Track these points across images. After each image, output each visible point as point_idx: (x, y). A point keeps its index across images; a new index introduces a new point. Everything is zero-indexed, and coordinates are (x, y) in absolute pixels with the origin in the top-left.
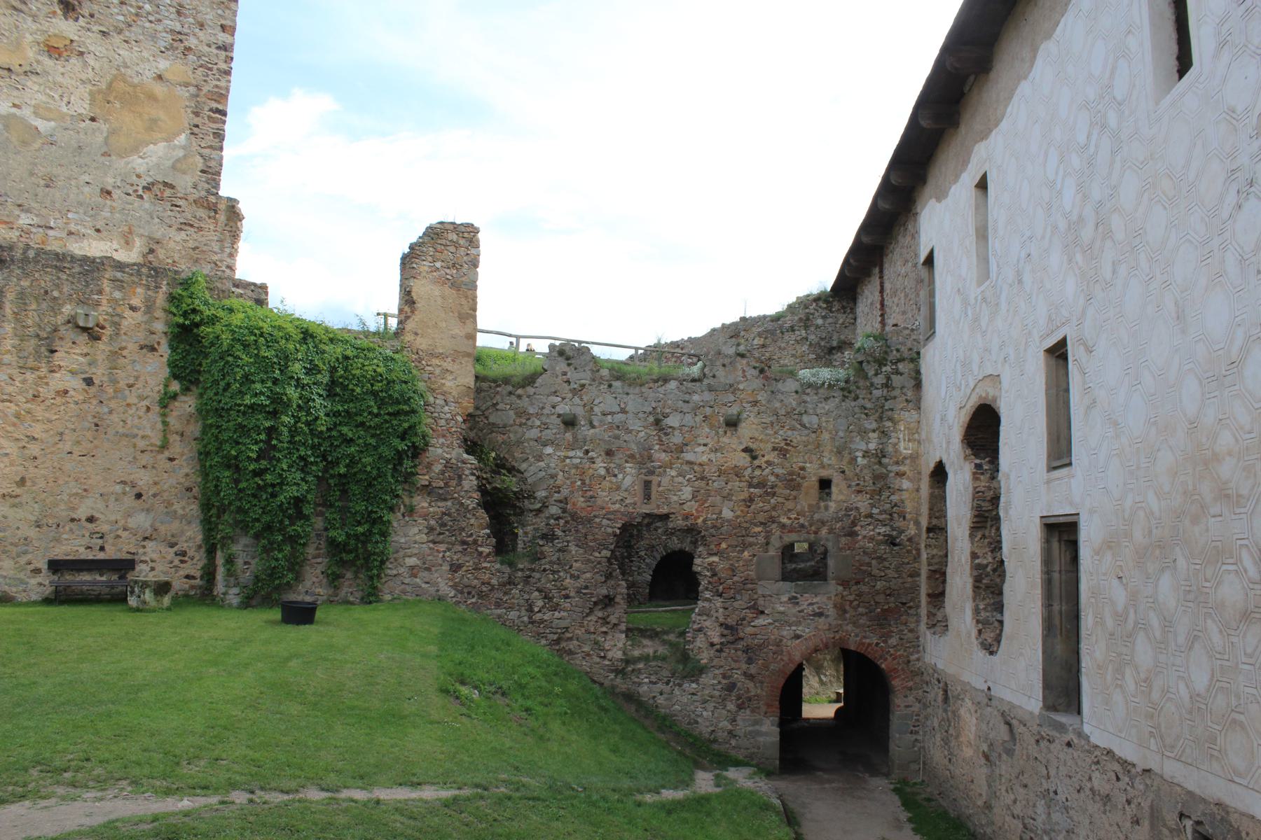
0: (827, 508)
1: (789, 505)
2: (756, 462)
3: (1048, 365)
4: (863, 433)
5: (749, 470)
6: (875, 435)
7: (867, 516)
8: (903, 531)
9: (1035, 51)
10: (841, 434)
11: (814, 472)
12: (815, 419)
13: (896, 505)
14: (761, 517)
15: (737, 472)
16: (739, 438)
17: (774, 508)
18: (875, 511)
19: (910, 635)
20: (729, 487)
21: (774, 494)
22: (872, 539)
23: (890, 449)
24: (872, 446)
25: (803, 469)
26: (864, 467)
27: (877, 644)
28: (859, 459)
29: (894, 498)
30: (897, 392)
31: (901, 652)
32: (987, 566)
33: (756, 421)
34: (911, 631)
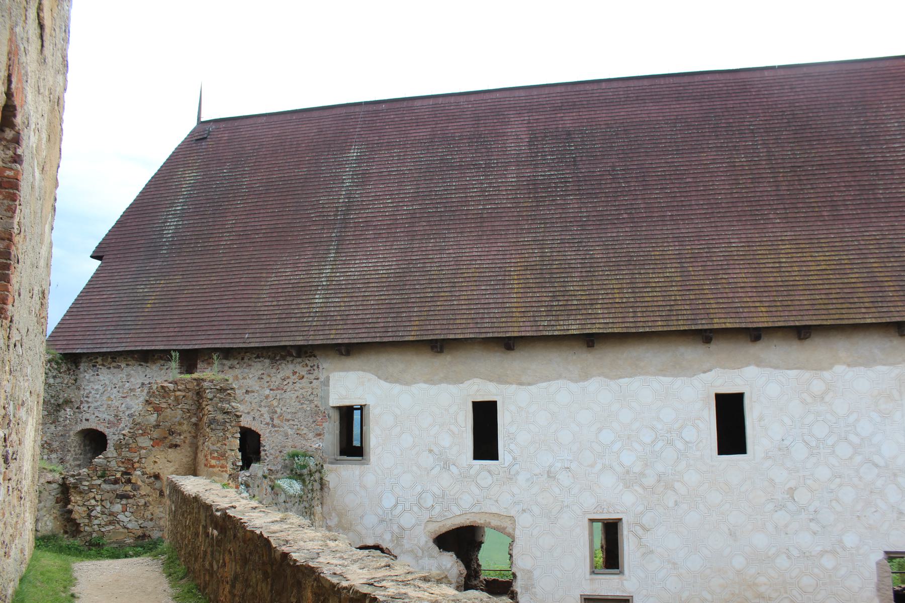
9: (585, 377)
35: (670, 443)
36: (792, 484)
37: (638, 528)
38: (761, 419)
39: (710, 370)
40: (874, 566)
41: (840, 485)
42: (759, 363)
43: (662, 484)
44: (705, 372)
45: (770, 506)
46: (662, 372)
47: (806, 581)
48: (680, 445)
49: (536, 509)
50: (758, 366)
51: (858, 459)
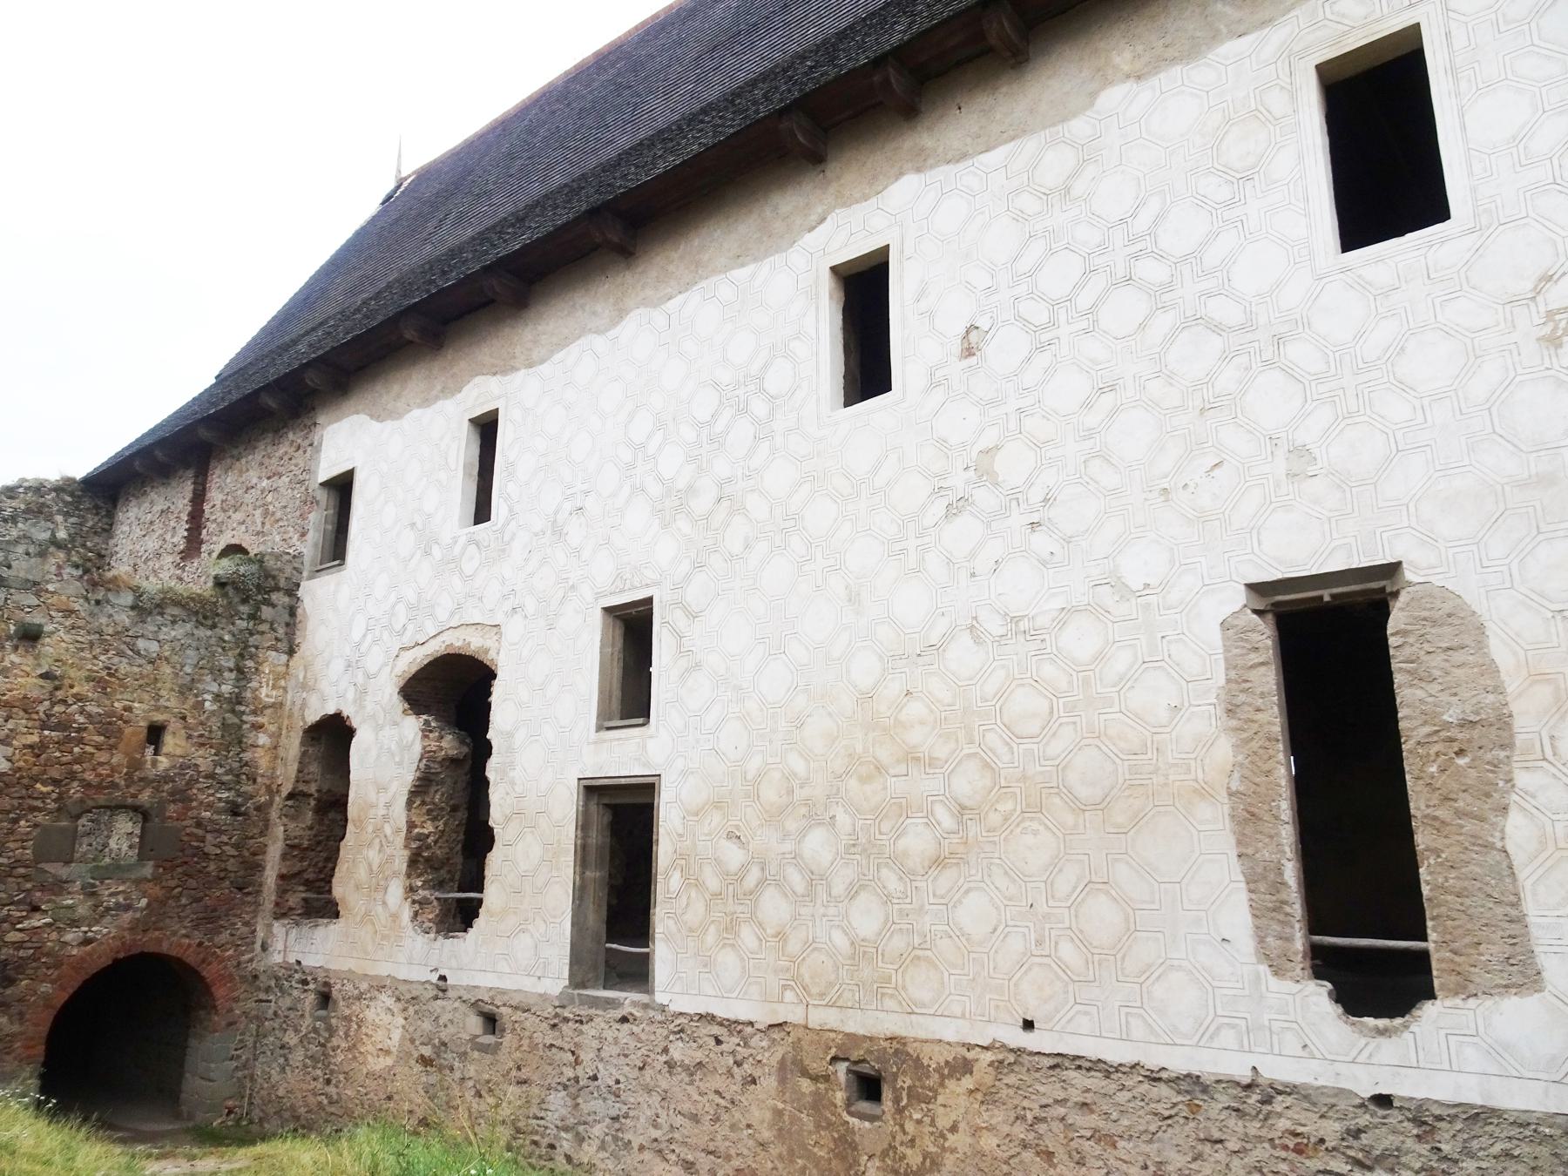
0: (154, 763)
1: (103, 757)
2: (60, 694)
3: (604, 625)
4: (217, 673)
5: (47, 703)
6: (233, 675)
7: (206, 777)
8: (252, 797)
10: (188, 669)
11: (142, 712)
12: (154, 647)
13: (246, 764)
14: (55, 773)
15: (27, 705)
16: (37, 657)
17: (78, 761)
18: (219, 771)
19: (245, 930)
20: (10, 725)
21: (80, 741)
22: (209, 806)
23: (248, 694)
24: (226, 689)
25: (128, 709)
26: (213, 713)
27: (200, 944)
28: (207, 704)
29: (247, 756)
30: (264, 627)
31: (231, 952)
32: (428, 836)
33: (67, 638)
34: (246, 924)
35: (743, 410)
36: (987, 441)
37: (679, 613)
38: (920, 296)
39: (823, 220)
40: (1216, 637)
41: (1114, 412)
42: (921, 161)
43: (725, 504)
44: (811, 229)
45: (939, 508)
46: (739, 259)
47: (1026, 704)
48: (759, 408)
49: (531, 606)
50: (918, 170)
51: (1164, 322)
